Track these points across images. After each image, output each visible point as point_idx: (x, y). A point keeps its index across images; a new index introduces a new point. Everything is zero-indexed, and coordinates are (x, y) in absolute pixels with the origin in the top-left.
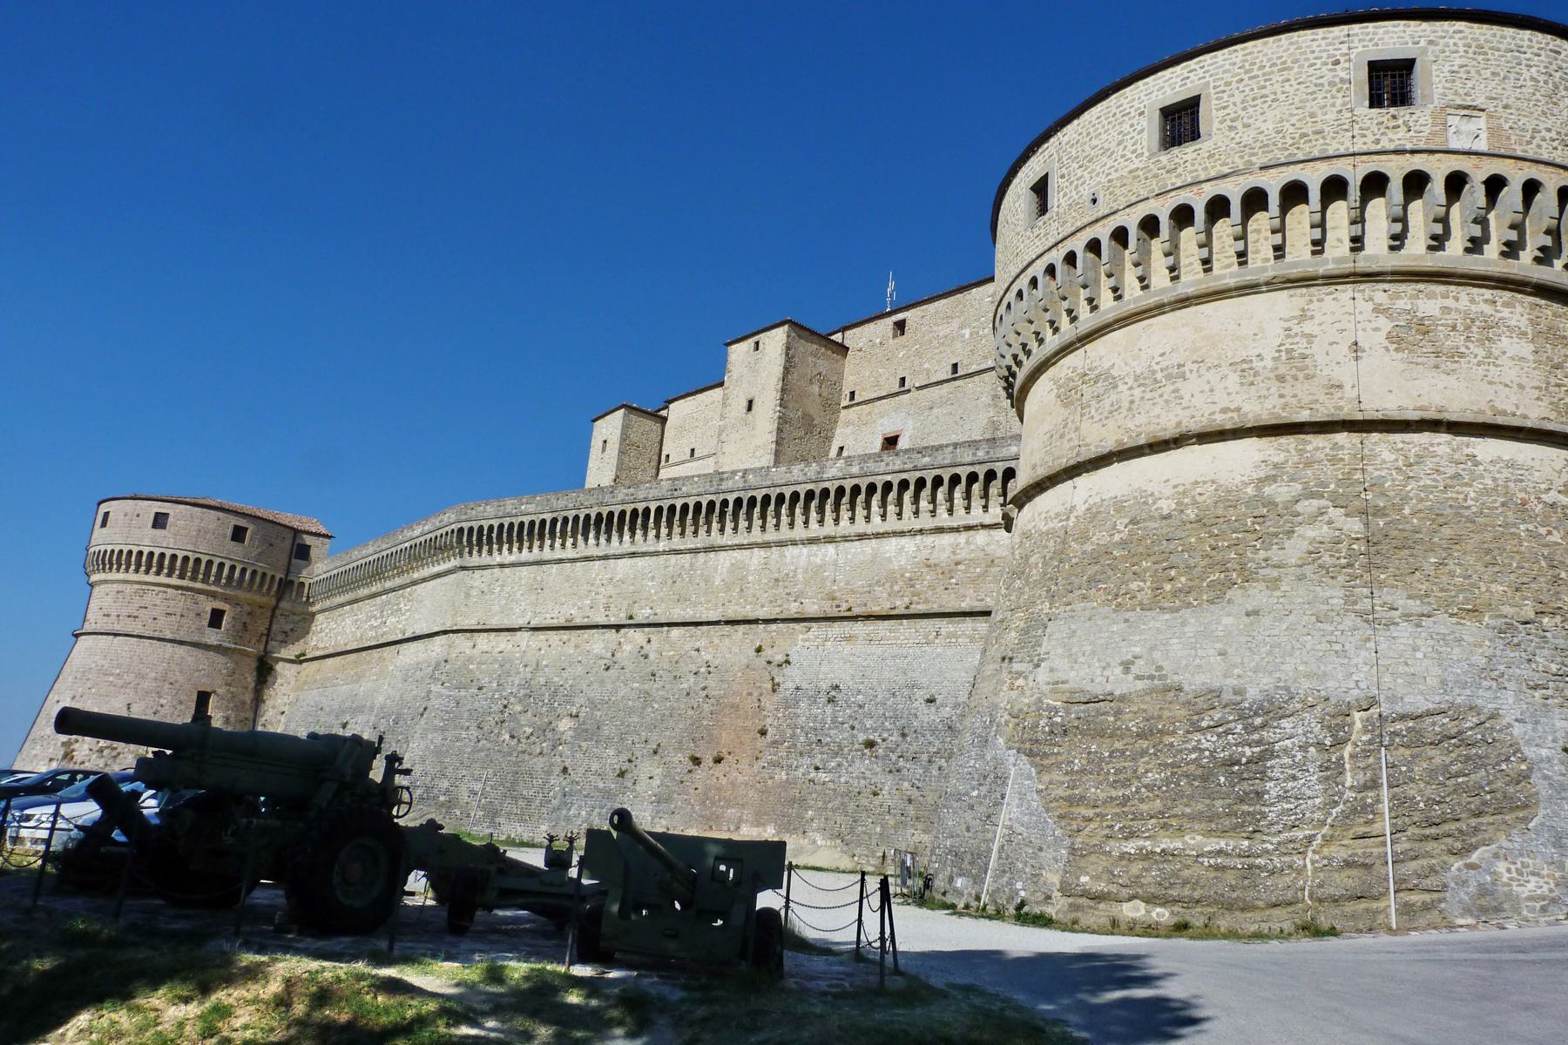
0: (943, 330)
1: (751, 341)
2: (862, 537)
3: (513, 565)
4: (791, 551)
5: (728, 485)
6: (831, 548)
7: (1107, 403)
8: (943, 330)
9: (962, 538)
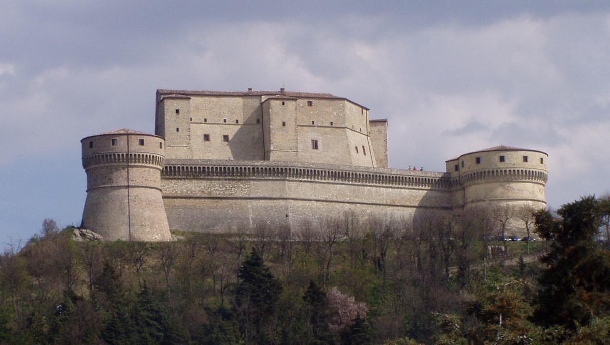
0: (327, 110)
1: (281, 102)
2: (398, 188)
3: (305, 181)
4: (382, 189)
5: (370, 171)
6: (391, 189)
7: (513, 191)
8: (327, 110)
9: (417, 191)
